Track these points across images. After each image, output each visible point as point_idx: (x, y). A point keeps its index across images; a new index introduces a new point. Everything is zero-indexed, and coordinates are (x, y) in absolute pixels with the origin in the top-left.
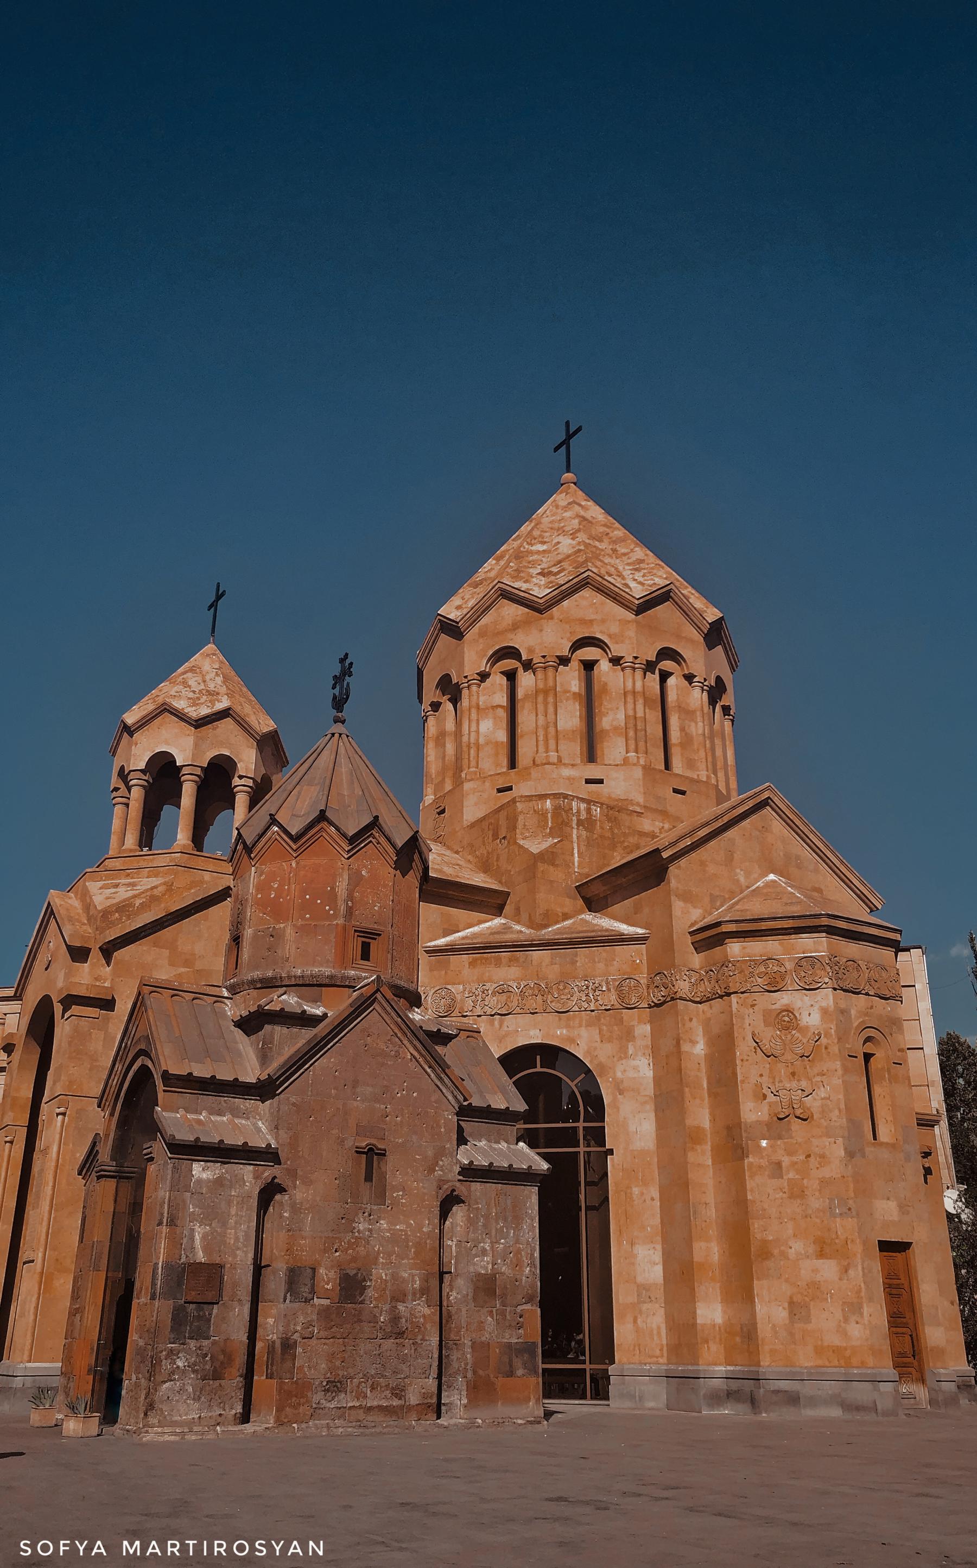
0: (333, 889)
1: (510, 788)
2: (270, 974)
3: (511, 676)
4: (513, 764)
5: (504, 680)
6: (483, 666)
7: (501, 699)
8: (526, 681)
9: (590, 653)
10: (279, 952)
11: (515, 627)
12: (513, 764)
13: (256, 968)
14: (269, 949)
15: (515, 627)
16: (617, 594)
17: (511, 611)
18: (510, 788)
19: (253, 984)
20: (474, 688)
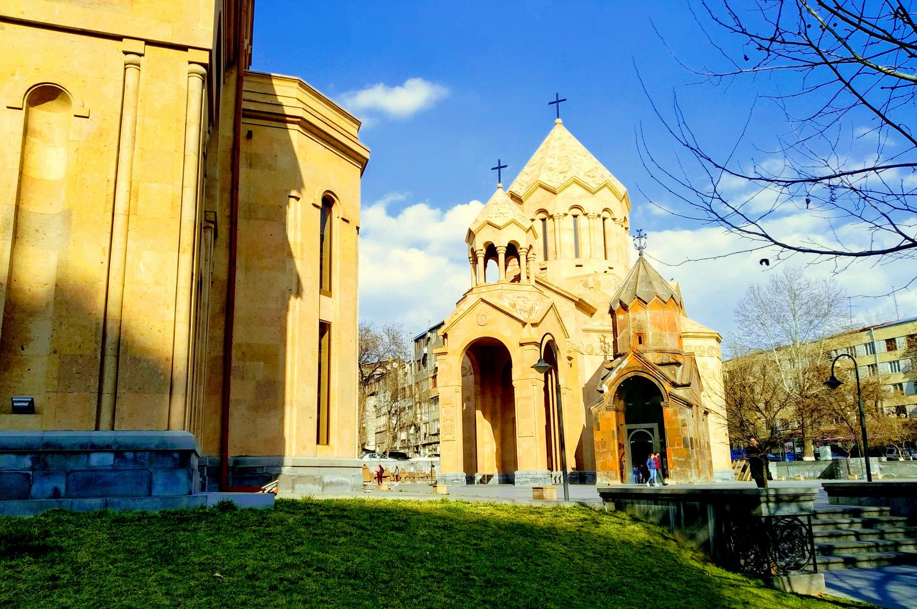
6: (567, 212)
9: (606, 214)
11: (580, 197)
12: (577, 256)
15: (580, 197)
17: (576, 190)
19: (656, 351)
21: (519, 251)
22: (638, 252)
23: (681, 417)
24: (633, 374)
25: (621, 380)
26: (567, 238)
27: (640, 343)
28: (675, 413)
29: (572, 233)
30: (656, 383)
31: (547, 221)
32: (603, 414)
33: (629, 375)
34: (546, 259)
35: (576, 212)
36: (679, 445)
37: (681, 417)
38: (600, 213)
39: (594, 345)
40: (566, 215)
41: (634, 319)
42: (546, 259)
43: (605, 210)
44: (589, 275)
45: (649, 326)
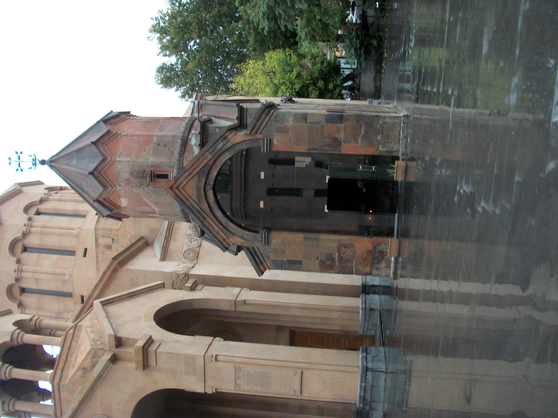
0: (143, 122)
1: (86, 250)
2: (179, 141)
3: (25, 249)
4: (72, 253)
5: (25, 255)
6: (15, 259)
7: (35, 256)
8: (33, 241)
9: (33, 210)
10: (168, 139)
12: (72, 253)
13: (172, 154)
14: (166, 146)
16: (10, 195)
18: (86, 250)
20: (24, 268)
21: (15, 343)
22: (39, 166)
23: (290, 123)
24: (210, 193)
25: (219, 214)
26: (48, 262)
27: (166, 176)
28: (284, 130)
29: (43, 255)
30: (227, 156)
31: (24, 285)
32: (275, 251)
33: (212, 199)
34: (69, 295)
35: (19, 248)
36: (338, 130)
37: (290, 123)
38: (27, 216)
39: (185, 248)
40: (18, 262)
41: (128, 181)
42: (69, 295)
43: (26, 209)
44: (96, 240)
45: (140, 160)
